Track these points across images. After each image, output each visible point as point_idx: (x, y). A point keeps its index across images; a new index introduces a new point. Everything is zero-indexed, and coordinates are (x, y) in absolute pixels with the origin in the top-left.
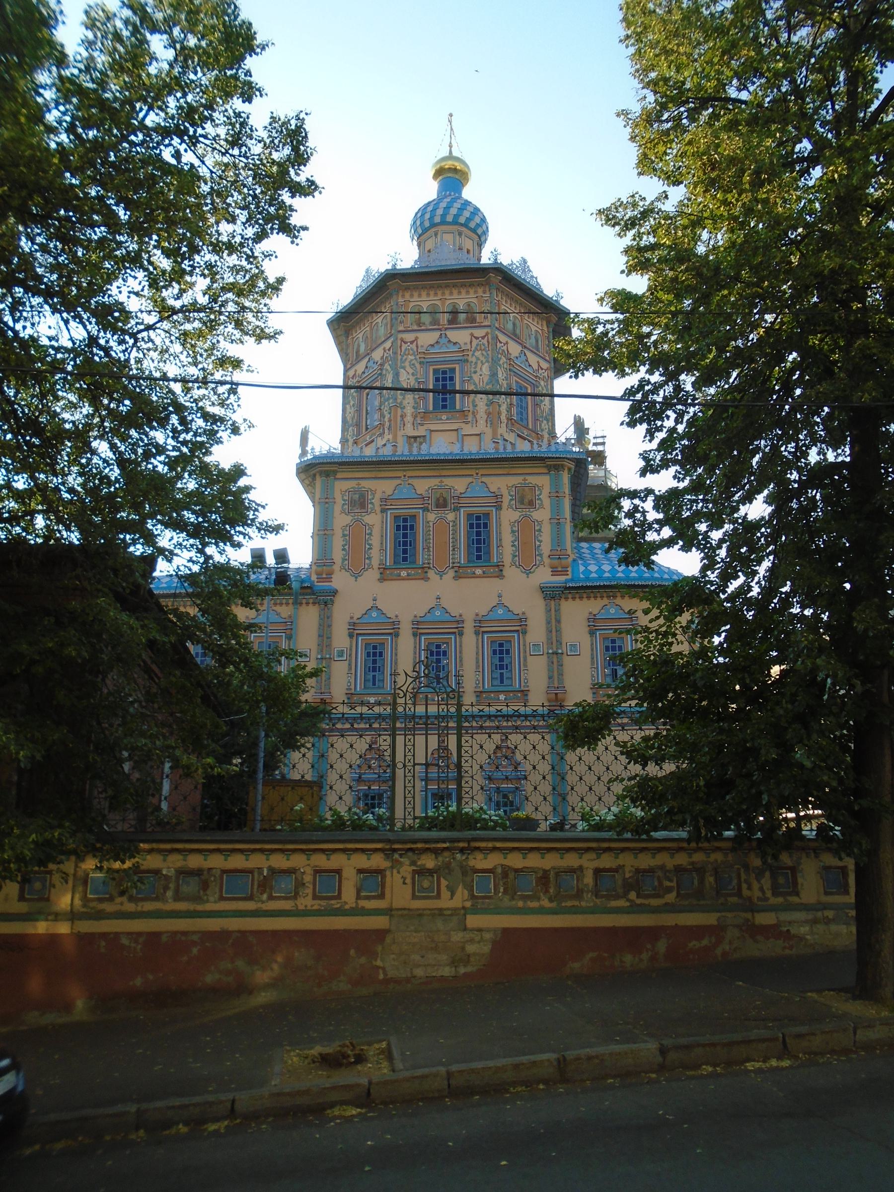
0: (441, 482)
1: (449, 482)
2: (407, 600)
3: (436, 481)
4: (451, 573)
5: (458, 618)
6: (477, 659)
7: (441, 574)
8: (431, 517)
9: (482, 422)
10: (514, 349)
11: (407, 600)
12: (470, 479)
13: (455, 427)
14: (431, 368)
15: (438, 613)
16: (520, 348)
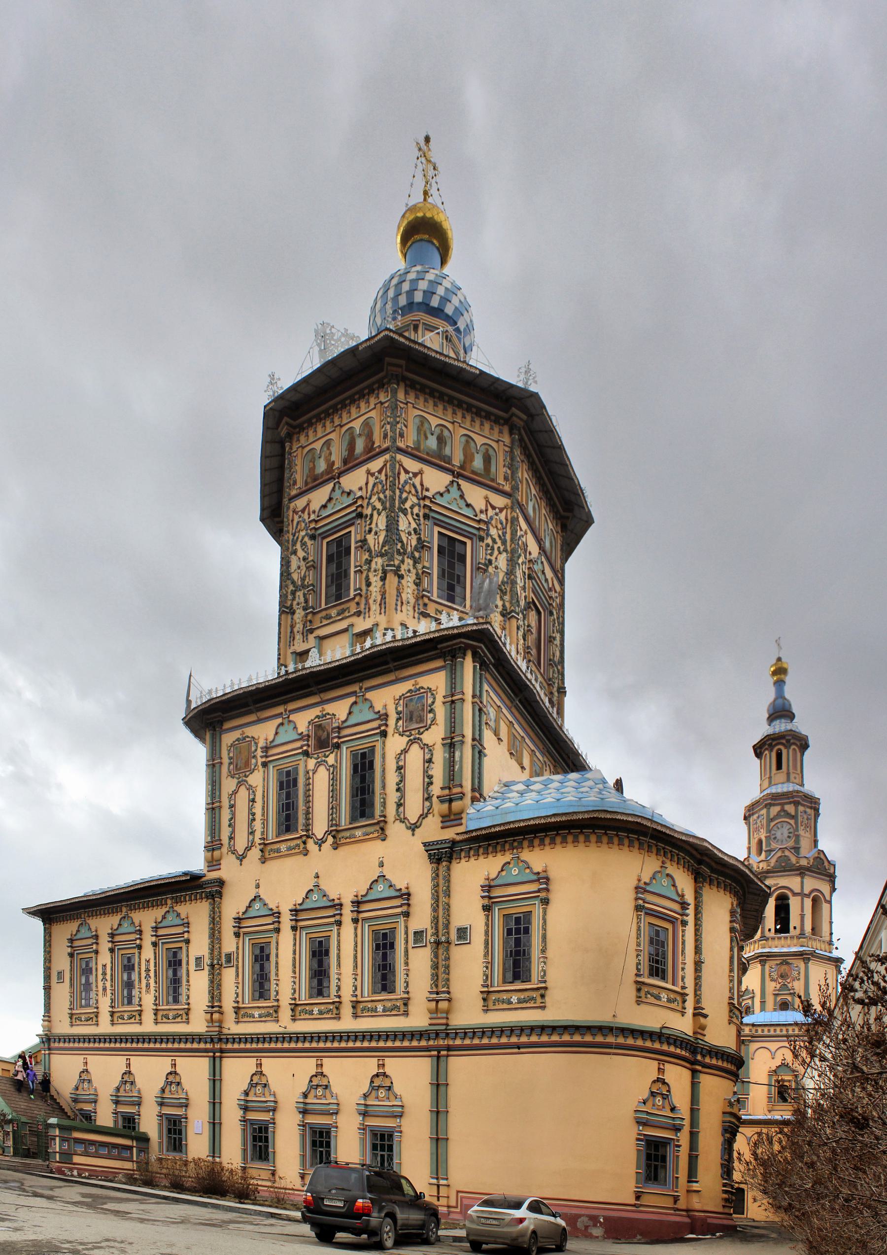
0: (323, 710)
1: (330, 708)
2: (284, 883)
3: (316, 711)
4: (330, 840)
5: (337, 902)
6: (356, 957)
7: (320, 843)
8: (311, 763)
9: (375, 607)
10: (435, 480)
11: (284, 883)
12: (353, 699)
13: (343, 625)
14: (325, 542)
15: (315, 896)
16: (449, 478)
